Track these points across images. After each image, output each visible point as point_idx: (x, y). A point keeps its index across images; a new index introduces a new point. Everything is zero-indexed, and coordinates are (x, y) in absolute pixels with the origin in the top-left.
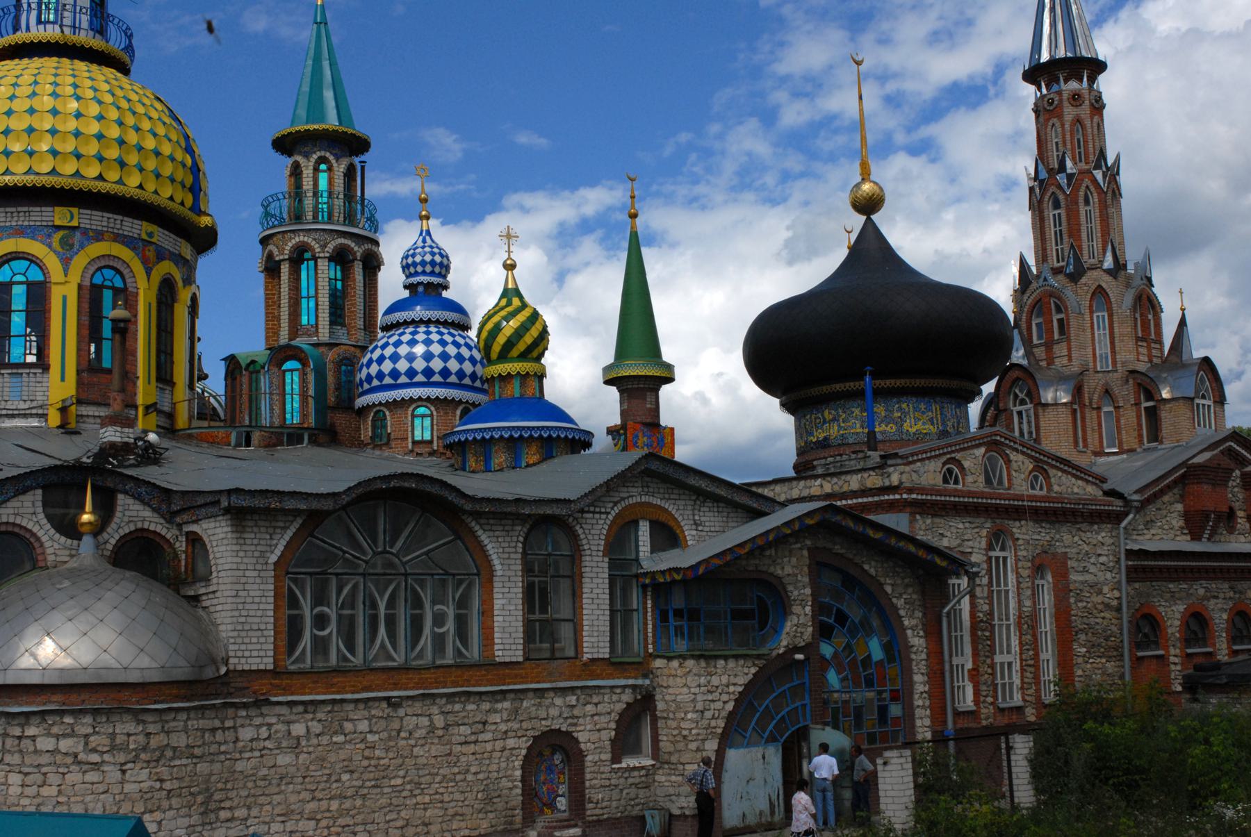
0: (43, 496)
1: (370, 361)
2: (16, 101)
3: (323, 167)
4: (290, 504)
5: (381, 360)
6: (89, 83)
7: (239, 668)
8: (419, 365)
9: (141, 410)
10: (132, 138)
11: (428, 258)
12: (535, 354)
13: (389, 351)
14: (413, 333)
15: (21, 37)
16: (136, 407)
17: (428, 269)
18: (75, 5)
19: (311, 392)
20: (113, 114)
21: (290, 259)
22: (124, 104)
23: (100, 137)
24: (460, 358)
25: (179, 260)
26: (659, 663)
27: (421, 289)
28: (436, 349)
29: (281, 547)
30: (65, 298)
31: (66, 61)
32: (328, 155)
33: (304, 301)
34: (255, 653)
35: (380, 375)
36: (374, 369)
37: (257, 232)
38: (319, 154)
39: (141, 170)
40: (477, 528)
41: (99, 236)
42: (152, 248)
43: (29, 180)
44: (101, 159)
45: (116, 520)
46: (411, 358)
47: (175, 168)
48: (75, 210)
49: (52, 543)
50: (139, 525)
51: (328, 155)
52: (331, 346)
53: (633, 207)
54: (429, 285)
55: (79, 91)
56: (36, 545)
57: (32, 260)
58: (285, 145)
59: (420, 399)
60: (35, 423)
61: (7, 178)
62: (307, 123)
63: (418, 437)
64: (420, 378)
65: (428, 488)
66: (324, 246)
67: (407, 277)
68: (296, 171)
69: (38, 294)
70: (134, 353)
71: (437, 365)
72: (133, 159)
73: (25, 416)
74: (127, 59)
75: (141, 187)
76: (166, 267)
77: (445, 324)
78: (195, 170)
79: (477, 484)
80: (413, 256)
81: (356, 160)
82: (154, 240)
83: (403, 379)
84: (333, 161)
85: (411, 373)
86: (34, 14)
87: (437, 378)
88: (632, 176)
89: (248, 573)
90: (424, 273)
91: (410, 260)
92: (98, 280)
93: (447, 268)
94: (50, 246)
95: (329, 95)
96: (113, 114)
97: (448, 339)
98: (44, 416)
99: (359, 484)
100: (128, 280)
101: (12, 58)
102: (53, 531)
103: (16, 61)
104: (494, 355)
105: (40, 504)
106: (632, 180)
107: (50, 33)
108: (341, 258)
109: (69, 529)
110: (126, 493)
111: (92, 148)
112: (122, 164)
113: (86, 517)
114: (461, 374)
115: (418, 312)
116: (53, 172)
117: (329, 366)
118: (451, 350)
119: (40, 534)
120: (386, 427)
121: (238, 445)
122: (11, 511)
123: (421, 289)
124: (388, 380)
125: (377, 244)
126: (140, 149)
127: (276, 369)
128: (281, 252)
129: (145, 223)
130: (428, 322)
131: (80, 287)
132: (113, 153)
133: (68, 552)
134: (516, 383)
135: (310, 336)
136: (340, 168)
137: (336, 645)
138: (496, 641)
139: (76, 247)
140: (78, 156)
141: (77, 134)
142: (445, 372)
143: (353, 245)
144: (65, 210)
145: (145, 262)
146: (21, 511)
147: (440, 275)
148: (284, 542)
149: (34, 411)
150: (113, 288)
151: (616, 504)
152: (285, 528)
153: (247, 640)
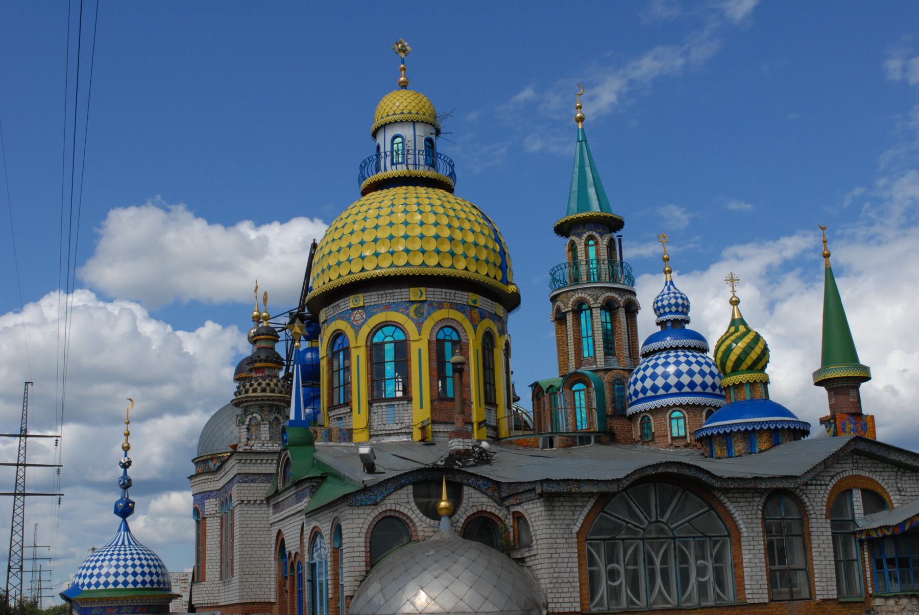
0: (414, 489)
1: (636, 380)
2: (380, 219)
3: (591, 242)
4: (586, 489)
5: (644, 378)
6: (427, 201)
7: (556, 611)
8: (673, 380)
9: (475, 426)
10: (458, 236)
11: (673, 301)
12: (759, 366)
13: (649, 372)
14: (666, 358)
15: (381, 175)
16: (472, 424)
17: (674, 309)
18: (415, 150)
19: (594, 405)
20: (445, 221)
21: (573, 311)
22: (452, 213)
23: (437, 237)
24: (703, 374)
25: (496, 318)
26: (878, 602)
27: (669, 324)
28: (684, 368)
29: (581, 521)
30: (420, 350)
31: (411, 188)
32: (594, 233)
33: (585, 340)
34: (567, 600)
35: (644, 390)
36: (639, 386)
37: (549, 293)
38: (588, 234)
39: (466, 257)
40: (725, 500)
41: (440, 306)
42: (476, 311)
43: (392, 271)
44: (438, 252)
45: (463, 505)
46: (666, 376)
47: (489, 254)
48: (423, 289)
49: (421, 523)
50: (480, 508)
51: (594, 233)
52: (606, 371)
53: (826, 249)
54: (675, 320)
55: (421, 208)
56: (411, 525)
57: (397, 326)
58: (563, 229)
59: (675, 405)
60: (404, 439)
61: (378, 271)
62: (578, 212)
63: (675, 434)
65: (686, 472)
66: (596, 300)
67: (659, 316)
68: (573, 247)
69: (402, 349)
70: (468, 386)
71: (685, 379)
72: (459, 250)
73: (398, 434)
74: (451, 181)
75: (466, 269)
76: (487, 324)
77: (689, 348)
78: (503, 253)
79: (722, 467)
80: (662, 300)
81: (615, 235)
82: (477, 305)
83: (661, 392)
84: (599, 238)
85: (667, 387)
86: (389, 159)
87: (686, 389)
88: (823, 226)
89: (558, 541)
90: (671, 312)
91: (660, 304)
92: (441, 336)
93: (688, 307)
94: (408, 315)
95: (592, 191)
96: (445, 221)
97: (693, 359)
98: (411, 433)
99: (635, 471)
100: (462, 335)
101: (376, 190)
102: (421, 515)
103: (379, 192)
104: (728, 370)
105: (411, 496)
106: (823, 229)
107: (400, 171)
108: (609, 307)
109: (432, 513)
110: (469, 485)
111: (432, 246)
112: (453, 254)
113: (443, 504)
114: (704, 385)
115: (669, 341)
116: (408, 264)
117: (606, 386)
118: (696, 368)
119: (413, 517)
120: (651, 428)
121: (544, 447)
122: (393, 501)
123: (669, 324)
124: (650, 393)
125: (634, 294)
126: (464, 242)
127: (568, 391)
128: (566, 305)
129: (470, 294)
130: (677, 349)
131: (429, 342)
132: (446, 247)
133: (432, 530)
134: (747, 390)
135: (590, 365)
136: (604, 242)
137: (626, 592)
138: (747, 587)
139: (425, 314)
140: (423, 252)
141: (422, 237)
142: (692, 385)
143: (617, 296)
144: (417, 289)
145: (472, 320)
146: (399, 501)
147: (682, 313)
148: (582, 517)
149: (403, 431)
150: (451, 341)
151: (832, 477)
152: (583, 507)
153: (560, 590)
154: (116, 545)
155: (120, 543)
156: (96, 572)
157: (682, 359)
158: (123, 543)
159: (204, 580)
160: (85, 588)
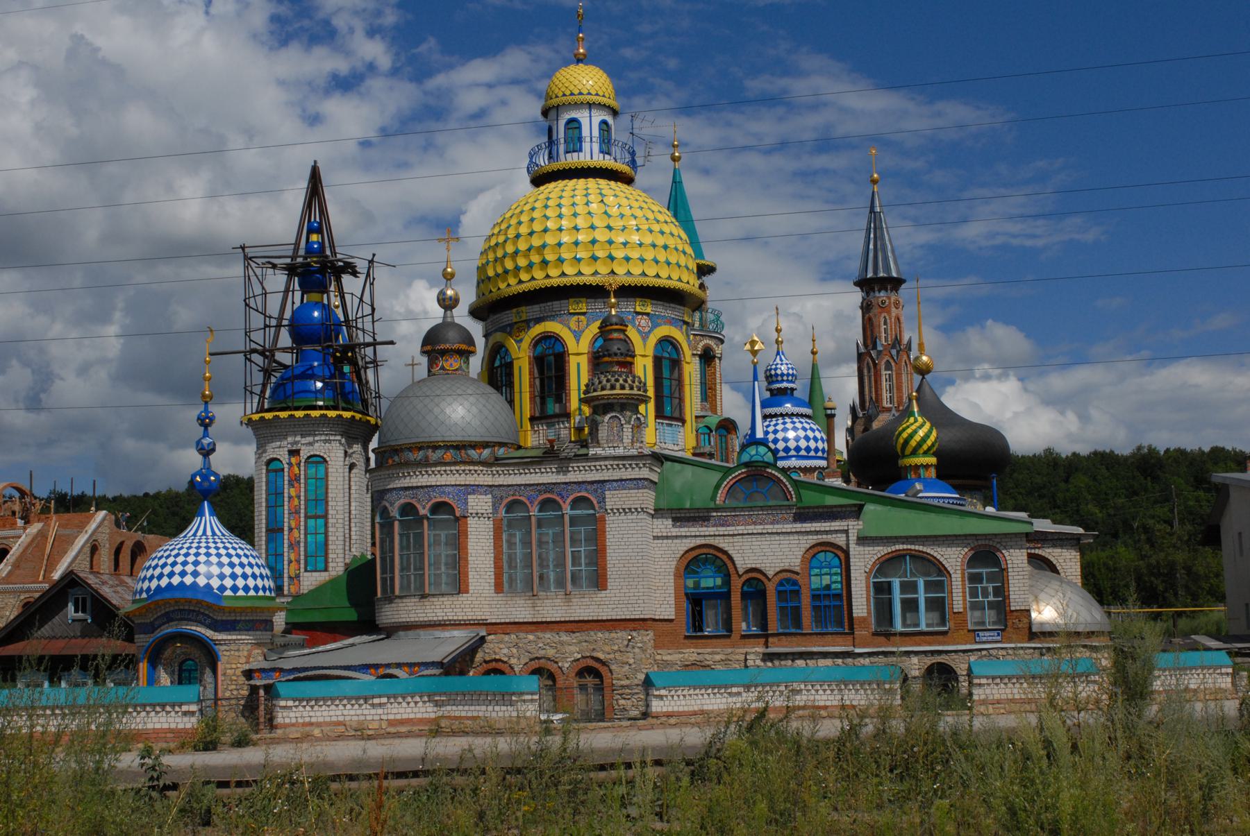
8: (792, 445)
46: (786, 440)
64: (793, 453)
67: (769, 383)
71: (803, 444)
77: (802, 416)
83: (812, 453)
97: (807, 426)
114: (808, 449)
124: (803, 453)
130: (791, 415)
154: (195, 535)
155: (200, 533)
156: (167, 570)
157: (798, 425)
158: (204, 533)
159: (467, 592)
160: (228, 593)
